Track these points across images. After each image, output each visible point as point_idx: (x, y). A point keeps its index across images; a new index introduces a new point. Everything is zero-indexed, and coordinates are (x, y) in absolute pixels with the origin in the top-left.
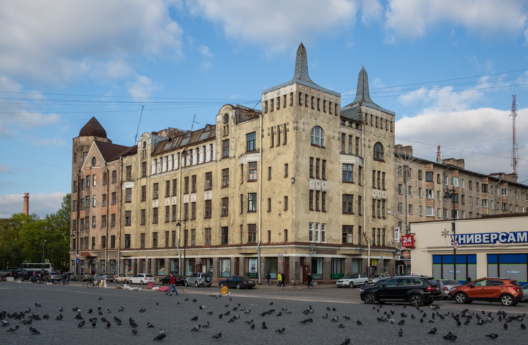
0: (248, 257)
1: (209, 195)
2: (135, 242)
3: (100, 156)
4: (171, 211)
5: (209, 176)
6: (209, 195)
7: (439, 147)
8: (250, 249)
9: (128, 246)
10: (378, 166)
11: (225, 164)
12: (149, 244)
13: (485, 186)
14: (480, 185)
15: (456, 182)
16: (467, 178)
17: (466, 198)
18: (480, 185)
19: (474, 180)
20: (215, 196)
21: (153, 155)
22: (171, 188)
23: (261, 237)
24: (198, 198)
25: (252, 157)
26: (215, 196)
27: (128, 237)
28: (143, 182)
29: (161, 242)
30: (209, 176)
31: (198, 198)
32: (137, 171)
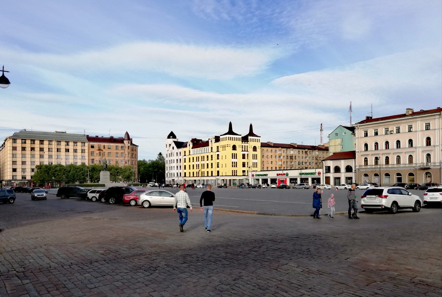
0: (218, 179)
1: (208, 162)
2: (187, 175)
3: (175, 147)
4: (198, 166)
5: (208, 156)
6: (208, 162)
7: (321, 125)
8: (218, 177)
9: (185, 176)
10: (255, 153)
11: (212, 154)
12: (192, 175)
13: (306, 152)
14: (304, 152)
15: (292, 152)
16: (297, 150)
17: (297, 157)
18: (304, 152)
19: (301, 150)
20: (210, 162)
21: (192, 148)
22: (198, 159)
23: (220, 174)
24: (205, 162)
25: (218, 153)
26: (210, 162)
27: (185, 173)
28: (190, 156)
29: (195, 175)
30: (208, 156)
31: (205, 162)
32: (187, 153)
